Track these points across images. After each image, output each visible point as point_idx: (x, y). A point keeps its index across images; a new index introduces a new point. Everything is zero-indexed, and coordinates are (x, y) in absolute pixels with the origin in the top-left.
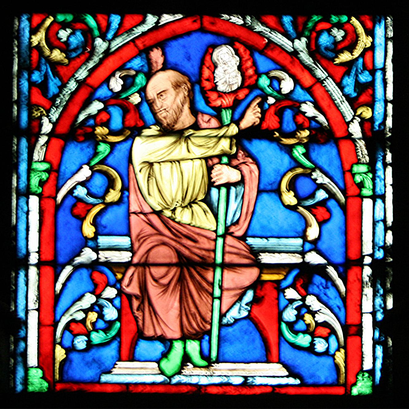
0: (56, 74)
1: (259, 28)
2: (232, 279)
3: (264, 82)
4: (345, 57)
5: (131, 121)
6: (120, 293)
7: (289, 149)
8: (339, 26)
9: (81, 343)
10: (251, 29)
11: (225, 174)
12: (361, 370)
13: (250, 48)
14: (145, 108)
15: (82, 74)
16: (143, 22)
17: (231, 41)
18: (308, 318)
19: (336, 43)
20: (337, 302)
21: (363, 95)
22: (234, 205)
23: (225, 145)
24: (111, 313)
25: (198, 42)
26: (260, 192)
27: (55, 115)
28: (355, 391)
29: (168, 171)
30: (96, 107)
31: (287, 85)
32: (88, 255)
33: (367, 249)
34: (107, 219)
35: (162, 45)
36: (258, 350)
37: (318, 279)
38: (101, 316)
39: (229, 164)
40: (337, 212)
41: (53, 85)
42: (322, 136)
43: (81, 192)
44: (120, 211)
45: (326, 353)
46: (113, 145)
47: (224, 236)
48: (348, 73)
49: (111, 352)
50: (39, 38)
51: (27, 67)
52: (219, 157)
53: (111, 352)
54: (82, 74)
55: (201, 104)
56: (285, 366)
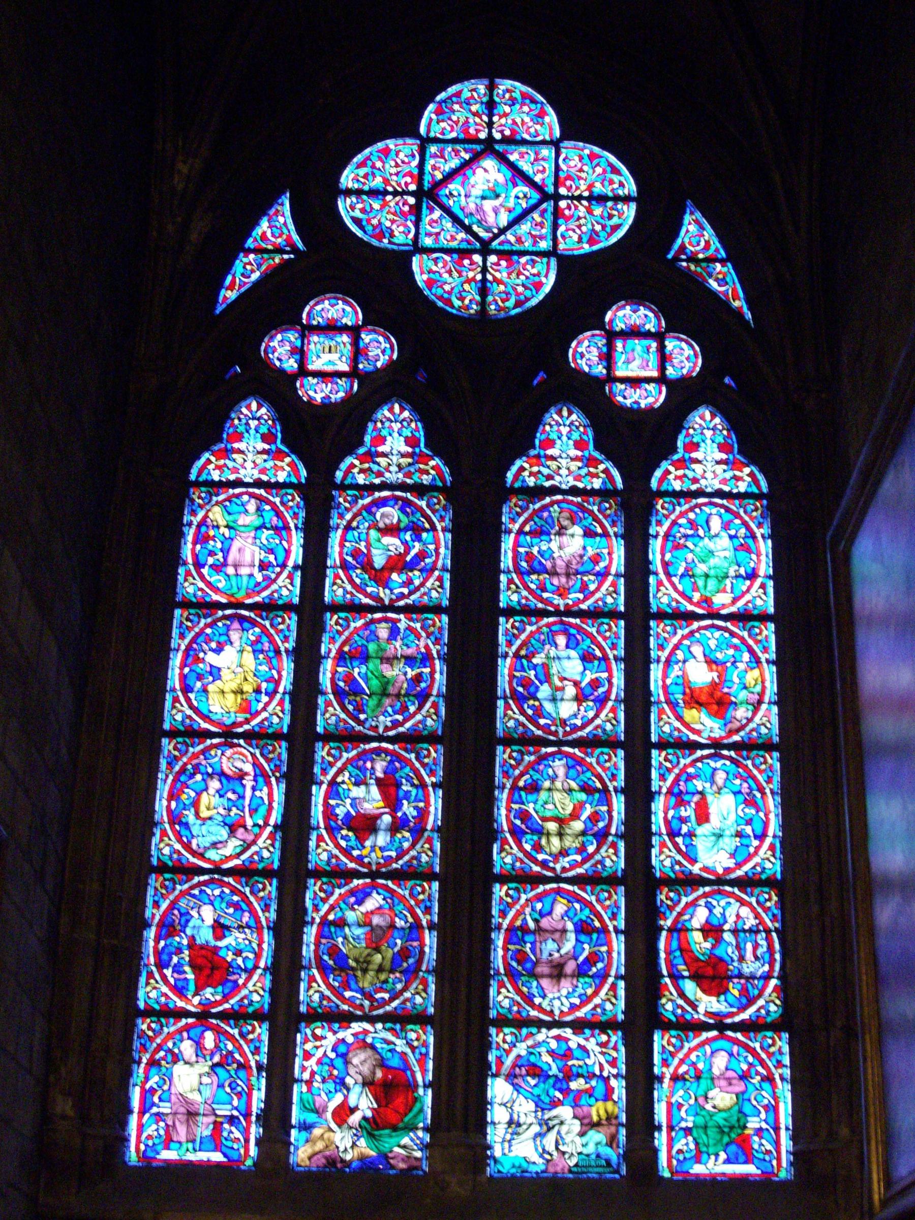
3: (222, 1045)
9: (150, 1143)
11: (206, 1080)
13: (218, 1031)
21: (257, 1051)
25: (198, 1030)
27: (148, 1056)
30: (162, 1054)
32: (155, 1110)
36: (212, 1146)
40: (244, 1095)
41: (148, 1044)
42: (241, 1066)
50: (144, 1027)
51: (139, 1037)
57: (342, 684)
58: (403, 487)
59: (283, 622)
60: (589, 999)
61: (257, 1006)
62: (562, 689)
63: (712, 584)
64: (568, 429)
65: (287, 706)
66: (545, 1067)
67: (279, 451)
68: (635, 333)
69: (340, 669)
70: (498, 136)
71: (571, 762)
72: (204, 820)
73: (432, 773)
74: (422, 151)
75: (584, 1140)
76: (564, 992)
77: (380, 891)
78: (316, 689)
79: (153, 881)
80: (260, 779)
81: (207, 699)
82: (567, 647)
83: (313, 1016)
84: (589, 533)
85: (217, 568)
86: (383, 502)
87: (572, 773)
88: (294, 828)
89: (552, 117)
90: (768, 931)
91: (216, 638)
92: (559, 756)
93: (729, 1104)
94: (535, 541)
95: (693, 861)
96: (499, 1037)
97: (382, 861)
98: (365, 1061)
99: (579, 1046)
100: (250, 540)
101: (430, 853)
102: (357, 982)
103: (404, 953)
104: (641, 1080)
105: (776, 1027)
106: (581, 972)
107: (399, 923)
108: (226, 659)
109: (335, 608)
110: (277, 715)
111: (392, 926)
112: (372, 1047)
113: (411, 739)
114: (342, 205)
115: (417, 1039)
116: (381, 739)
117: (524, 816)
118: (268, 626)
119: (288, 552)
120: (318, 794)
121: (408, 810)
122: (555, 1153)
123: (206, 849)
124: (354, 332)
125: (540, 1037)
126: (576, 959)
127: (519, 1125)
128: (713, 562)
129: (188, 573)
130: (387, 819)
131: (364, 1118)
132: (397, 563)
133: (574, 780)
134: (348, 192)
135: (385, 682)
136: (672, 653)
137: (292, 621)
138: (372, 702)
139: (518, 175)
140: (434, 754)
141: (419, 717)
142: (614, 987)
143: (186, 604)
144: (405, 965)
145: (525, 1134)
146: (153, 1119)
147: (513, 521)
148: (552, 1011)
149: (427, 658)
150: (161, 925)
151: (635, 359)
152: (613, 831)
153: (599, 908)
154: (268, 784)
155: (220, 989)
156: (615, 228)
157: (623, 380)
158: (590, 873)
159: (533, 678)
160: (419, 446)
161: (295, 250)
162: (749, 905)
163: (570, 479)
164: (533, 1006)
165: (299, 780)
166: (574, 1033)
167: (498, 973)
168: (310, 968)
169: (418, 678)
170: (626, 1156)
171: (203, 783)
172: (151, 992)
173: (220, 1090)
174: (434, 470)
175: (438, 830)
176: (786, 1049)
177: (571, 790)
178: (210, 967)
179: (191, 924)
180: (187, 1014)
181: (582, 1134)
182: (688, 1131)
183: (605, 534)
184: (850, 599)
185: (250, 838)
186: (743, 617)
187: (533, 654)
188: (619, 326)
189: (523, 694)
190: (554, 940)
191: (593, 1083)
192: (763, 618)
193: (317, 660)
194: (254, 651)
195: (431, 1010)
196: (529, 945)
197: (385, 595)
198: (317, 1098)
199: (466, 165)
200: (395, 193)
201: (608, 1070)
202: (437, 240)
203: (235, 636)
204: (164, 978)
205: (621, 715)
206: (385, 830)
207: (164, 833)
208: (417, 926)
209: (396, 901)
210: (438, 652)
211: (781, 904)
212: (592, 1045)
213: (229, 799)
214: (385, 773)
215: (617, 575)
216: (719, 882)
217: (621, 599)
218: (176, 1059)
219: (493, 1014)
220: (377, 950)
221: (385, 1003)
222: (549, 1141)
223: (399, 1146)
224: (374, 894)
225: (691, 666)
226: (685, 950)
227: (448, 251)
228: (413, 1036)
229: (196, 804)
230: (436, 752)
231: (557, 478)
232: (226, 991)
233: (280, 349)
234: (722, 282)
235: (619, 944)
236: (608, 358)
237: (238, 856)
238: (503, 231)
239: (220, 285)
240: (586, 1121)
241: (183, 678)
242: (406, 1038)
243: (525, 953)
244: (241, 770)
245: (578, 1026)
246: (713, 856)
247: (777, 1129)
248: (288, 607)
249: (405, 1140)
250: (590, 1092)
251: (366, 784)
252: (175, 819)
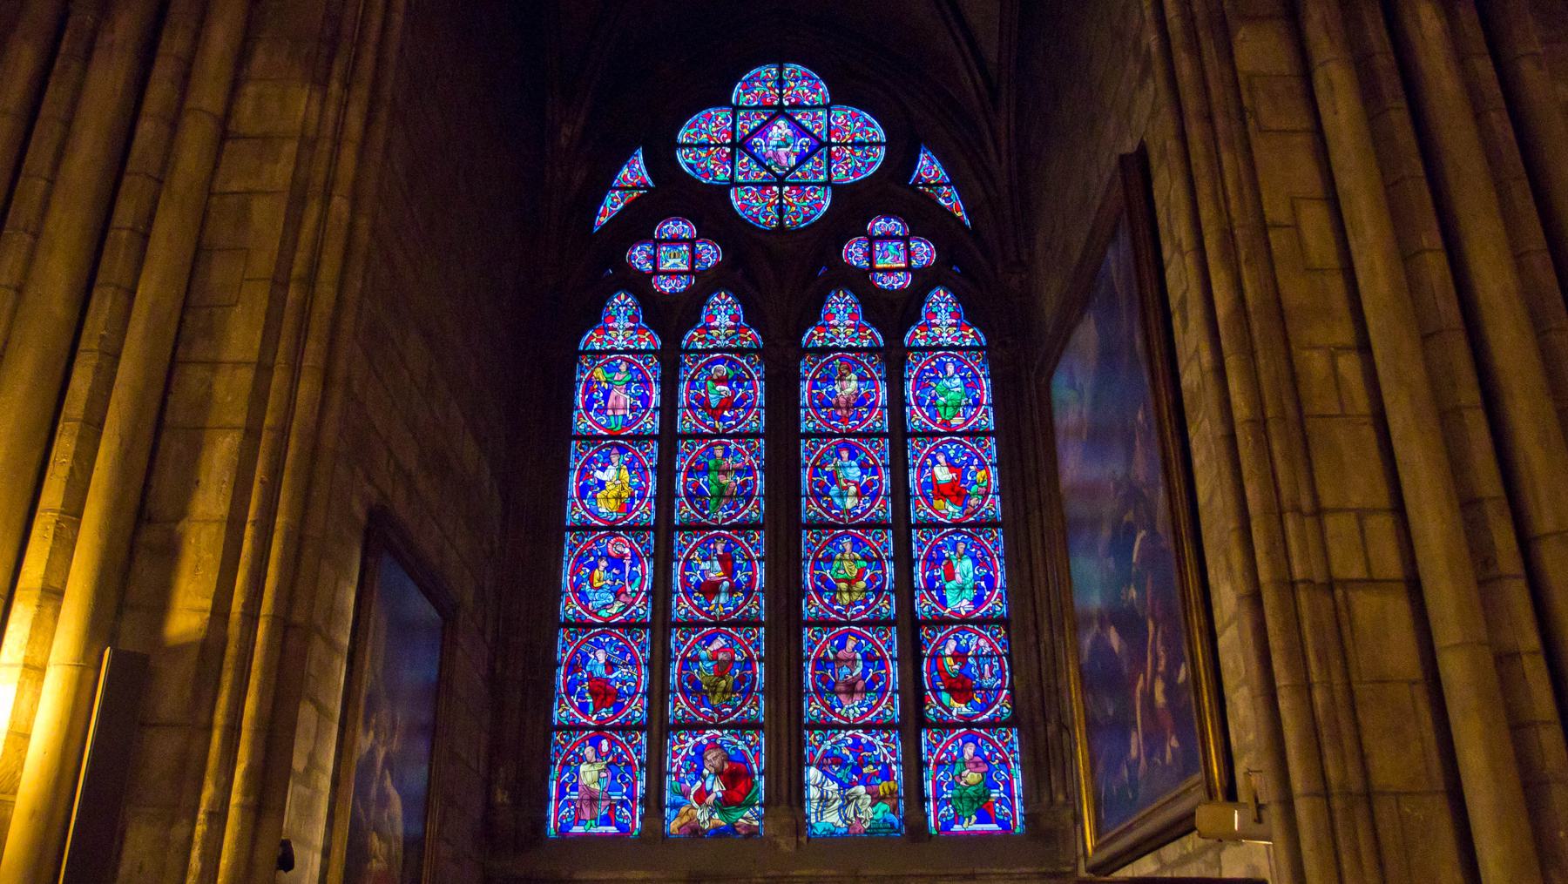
13: (613, 742)
29: (590, 774)
58: (729, 350)
63: (950, 411)
67: (641, 328)
68: (888, 237)
70: (786, 103)
73: (757, 551)
74: (734, 116)
78: (673, 495)
79: (562, 633)
83: (677, 727)
84: (861, 379)
85: (602, 411)
88: (661, 593)
89: (823, 88)
90: (1000, 656)
93: (976, 781)
95: (944, 606)
96: (812, 737)
103: (742, 679)
104: (914, 767)
105: (1008, 724)
106: (869, 687)
107: (738, 658)
108: (608, 475)
109: (685, 436)
110: (645, 513)
111: (733, 659)
112: (721, 746)
113: (741, 527)
114: (680, 156)
116: (720, 527)
119: (649, 399)
120: (677, 568)
121: (741, 576)
124: (691, 243)
125: (841, 736)
127: (827, 800)
128: (950, 395)
129: (580, 415)
130: (726, 583)
132: (728, 404)
134: (684, 146)
135: (722, 488)
136: (924, 460)
137: (654, 447)
139: (800, 130)
142: (891, 699)
143: (579, 437)
145: (831, 807)
147: (808, 371)
149: (750, 471)
151: (891, 256)
154: (642, 562)
156: (872, 164)
157: (881, 270)
161: (647, 186)
162: (985, 637)
164: (835, 714)
165: (664, 559)
167: (808, 691)
169: (745, 484)
170: (904, 821)
172: (562, 713)
174: (751, 338)
175: (763, 591)
176: (1016, 739)
177: (855, 560)
178: (605, 693)
180: (587, 727)
181: (872, 805)
182: (948, 801)
183: (873, 379)
184: (1051, 418)
185: (629, 600)
186: (973, 434)
188: (878, 232)
189: (820, 493)
192: (987, 434)
193: (674, 473)
197: (719, 426)
199: (764, 124)
200: (716, 145)
201: (890, 759)
202: (746, 177)
203: (614, 458)
204: (572, 705)
207: (569, 599)
208: (749, 661)
211: (1008, 636)
212: (877, 741)
215: (883, 407)
216: (963, 622)
218: (582, 760)
219: (806, 720)
221: (729, 715)
222: (850, 811)
225: (936, 469)
226: (942, 671)
227: (755, 185)
229: (590, 578)
233: (639, 256)
234: (948, 199)
235: (893, 668)
236: (870, 256)
237: (621, 613)
238: (792, 169)
239: (596, 214)
245: (867, 728)
246: (959, 603)
247: (1012, 797)
248: (651, 437)
249: (747, 814)
252: (576, 588)
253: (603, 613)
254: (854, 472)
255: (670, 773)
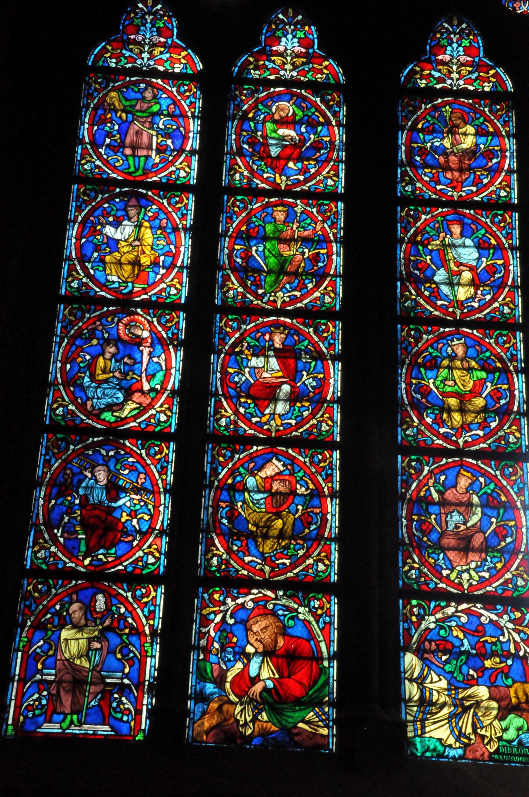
0: (35, 602)
1: (114, 587)
2: (93, 689)
3: (114, 608)
4: (145, 600)
5: (62, 622)
6: (49, 693)
7: (120, 636)
8: (144, 588)
9: (30, 715)
10: (111, 587)
12: (140, 729)
13: (109, 596)
14: (68, 617)
15: (45, 603)
16: (71, 583)
17: (103, 592)
18: (122, 706)
19: (142, 594)
20: (133, 700)
21: (151, 615)
22: (97, 658)
23: (96, 633)
24: (44, 702)
25: (89, 592)
26: (108, 653)
28: (137, 738)
29: (73, 642)
30: (49, 616)
31: (123, 610)
32: (39, 677)
33: (147, 678)
34: (48, 661)
35: (76, 592)
36: (100, 720)
37: (127, 690)
38: (40, 703)
39: (97, 642)
40: (136, 662)
43: (39, 650)
44: (53, 659)
45: (127, 722)
46: (53, 632)
47: (92, 671)
48: (146, 606)
49: (42, 719)
50: (30, 588)
51: (25, 599)
52: (94, 638)
53: (42, 719)
54: (45, 603)
55: (89, 616)
56: (111, 727)
57: (239, 260)
59: (181, 201)
60: (500, 573)
61: (152, 568)
62: (459, 273)
64: (458, 36)
65: (185, 279)
66: (457, 643)
69: (236, 247)
71: (470, 342)
72: (100, 383)
75: (504, 724)
76: (473, 565)
77: (280, 457)
80: (159, 347)
81: (105, 269)
82: (462, 235)
84: (480, 132)
85: (113, 148)
86: (278, 97)
87: (471, 352)
91: (113, 213)
92: (457, 336)
94: (428, 137)
97: (281, 428)
98: (266, 628)
99: (491, 621)
100: (147, 125)
101: (330, 423)
102: (257, 547)
103: (306, 520)
107: (301, 490)
111: (293, 493)
112: (273, 613)
113: (312, 315)
115: (321, 607)
117: (426, 392)
118: (166, 204)
120: (216, 362)
122: (472, 737)
123: (102, 411)
125: (450, 611)
126: (484, 533)
127: (432, 704)
129: (85, 151)
130: (286, 388)
131: (265, 689)
133: (474, 359)
135: (283, 261)
137: (191, 201)
138: (270, 279)
140: (332, 329)
141: (317, 294)
143: (84, 179)
144: (307, 531)
146: (35, 688)
148: (460, 584)
149: (324, 240)
150: (52, 484)
152: (515, 408)
153: (505, 483)
155: (113, 551)
158: (493, 448)
159: (429, 261)
160: (313, 47)
163: (461, 82)
164: (441, 578)
166: (484, 608)
168: (208, 532)
169: (316, 258)
171: (99, 347)
173: (111, 657)
174: (329, 70)
175: (339, 401)
179: (84, 485)
187: (429, 240)
190: (458, 512)
191: (509, 662)
194: (151, 228)
195: (334, 578)
196: (433, 516)
197: (282, 181)
198: (216, 667)
203: (132, 212)
205: (519, 300)
206: (285, 401)
207: (58, 394)
208: (317, 493)
209: (297, 469)
210: (335, 235)
212: (504, 621)
213: (125, 364)
214: (283, 344)
217: (515, 194)
220: (278, 515)
223: (303, 721)
224: (274, 461)
228: (317, 604)
229: (91, 366)
230: (334, 327)
231: (449, 82)
232: (119, 553)
240: (504, 703)
241: (79, 248)
242: (308, 606)
243: (430, 523)
244: (138, 337)
245: (490, 601)
248: (186, 188)
250: (506, 672)
251: (267, 357)
252: (71, 381)
253: (108, 416)
254: (469, 254)
255: (198, 648)
